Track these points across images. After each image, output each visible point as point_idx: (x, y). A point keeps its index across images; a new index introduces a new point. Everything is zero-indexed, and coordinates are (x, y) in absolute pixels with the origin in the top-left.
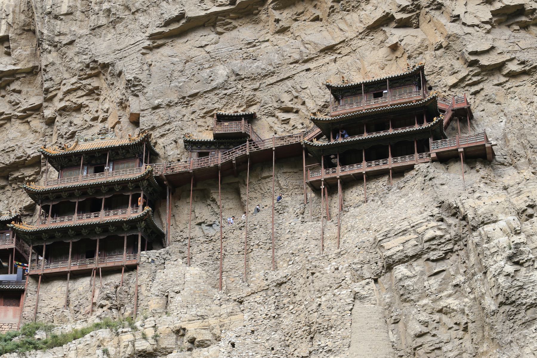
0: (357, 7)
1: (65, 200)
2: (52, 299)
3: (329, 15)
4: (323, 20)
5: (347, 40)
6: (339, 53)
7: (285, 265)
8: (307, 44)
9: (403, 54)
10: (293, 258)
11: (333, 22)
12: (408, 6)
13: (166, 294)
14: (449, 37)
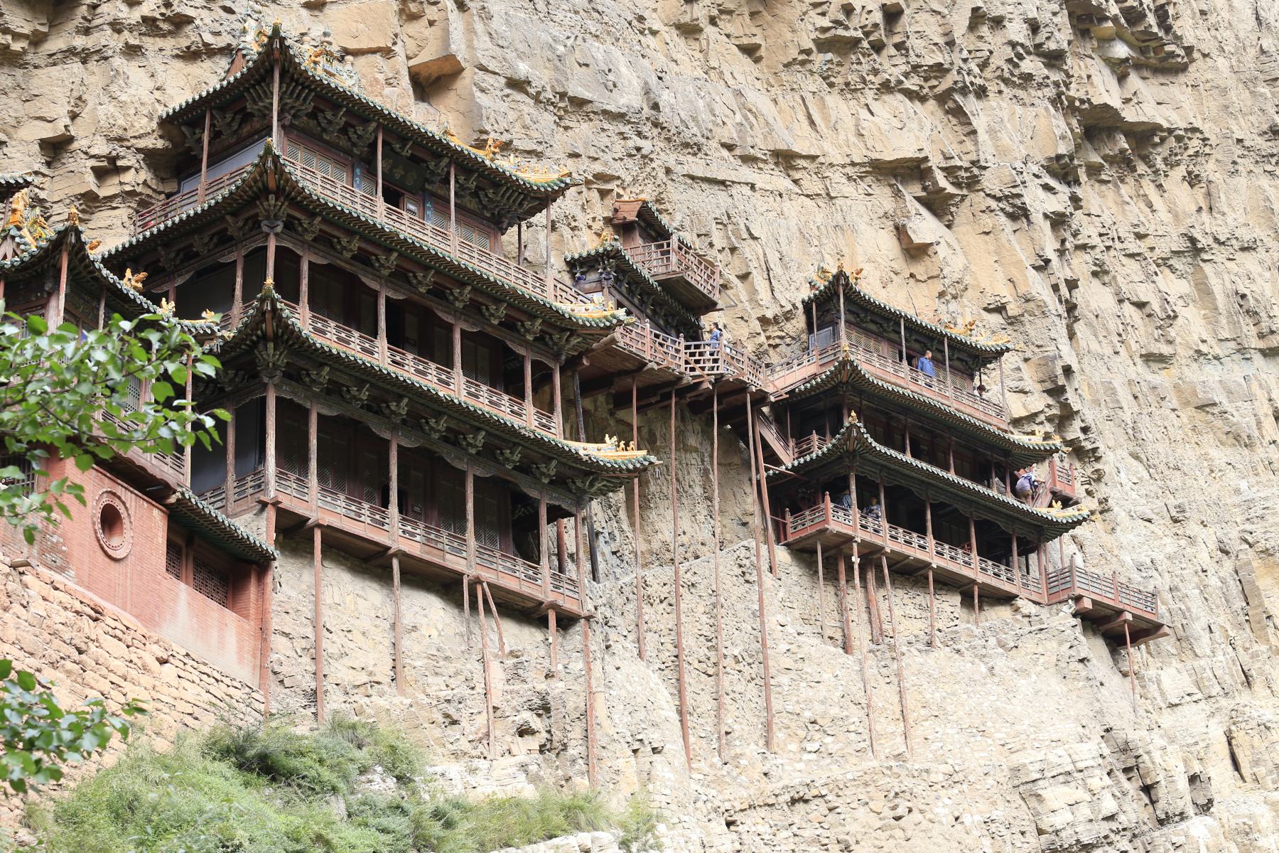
0: (856, 90)
1: (343, 264)
2: (349, 635)
3: (787, 65)
4: (764, 62)
5: (821, 159)
6: (796, 182)
7: (794, 747)
8: (750, 111)
9: (929, 278)
10: (817, 736)
11: (792, 90)
12: (960, 168)
13: (636, 745)
14: (1027, 301)
